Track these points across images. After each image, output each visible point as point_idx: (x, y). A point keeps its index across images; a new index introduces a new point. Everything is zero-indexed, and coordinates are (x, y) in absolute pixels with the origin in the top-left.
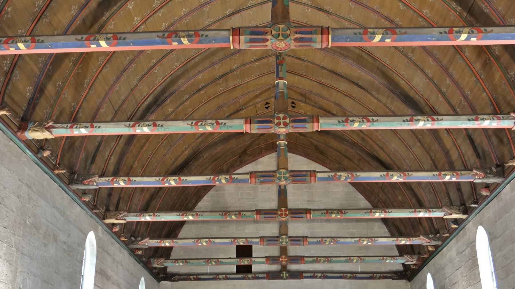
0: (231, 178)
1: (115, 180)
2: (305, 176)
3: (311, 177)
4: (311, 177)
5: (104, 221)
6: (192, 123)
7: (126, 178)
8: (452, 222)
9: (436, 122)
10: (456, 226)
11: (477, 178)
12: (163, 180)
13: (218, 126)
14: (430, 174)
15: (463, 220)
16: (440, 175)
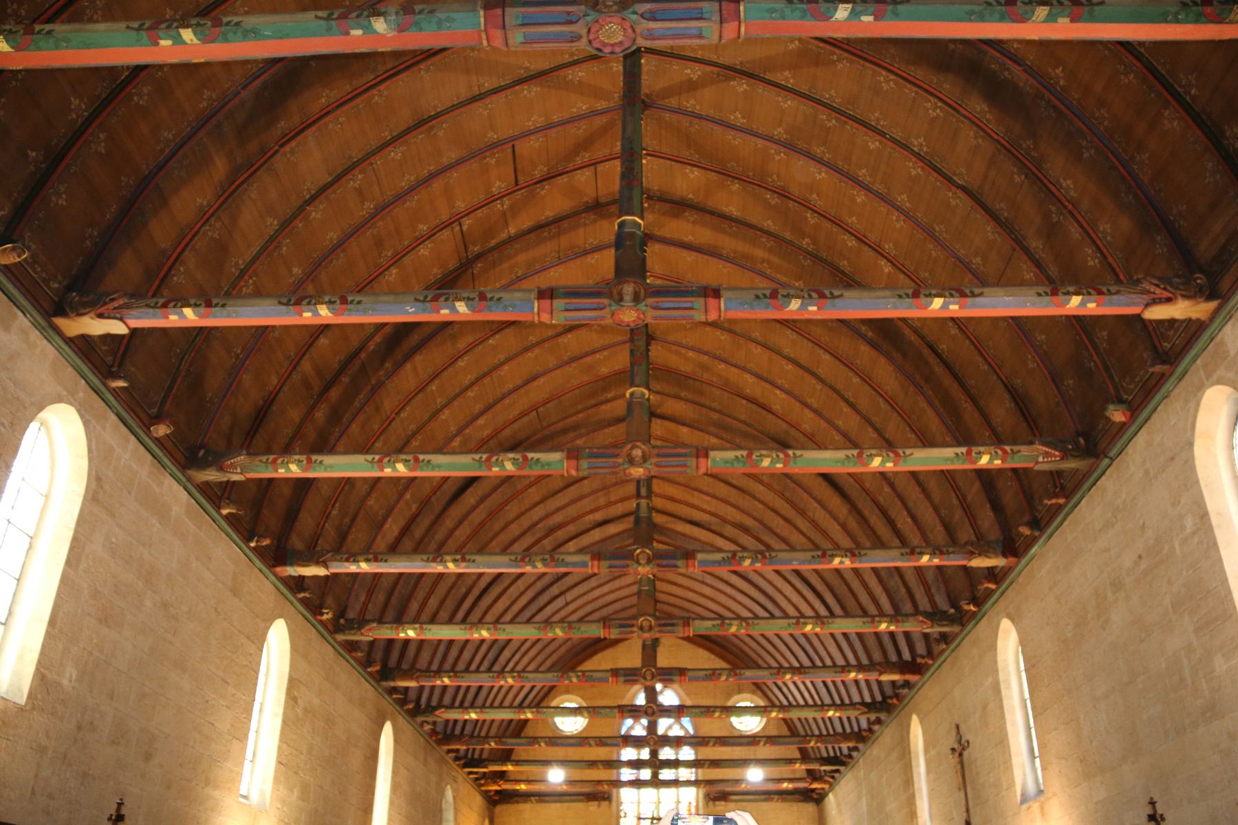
0: (525, 458)
1: (280, 461)
2: (685, 455)
3: (697, 457)
4: (697, 457)
5: (278, 569)
6: (426, 297)
7: (303, 458)
8: (986, 578)
9: (970, 300)
10: (992, 586)
11: (1041, 459)
12: (380, 461)
13: (483, 303)
14: (949, 452)
15: (1006, 572)
16: (969, 453)
